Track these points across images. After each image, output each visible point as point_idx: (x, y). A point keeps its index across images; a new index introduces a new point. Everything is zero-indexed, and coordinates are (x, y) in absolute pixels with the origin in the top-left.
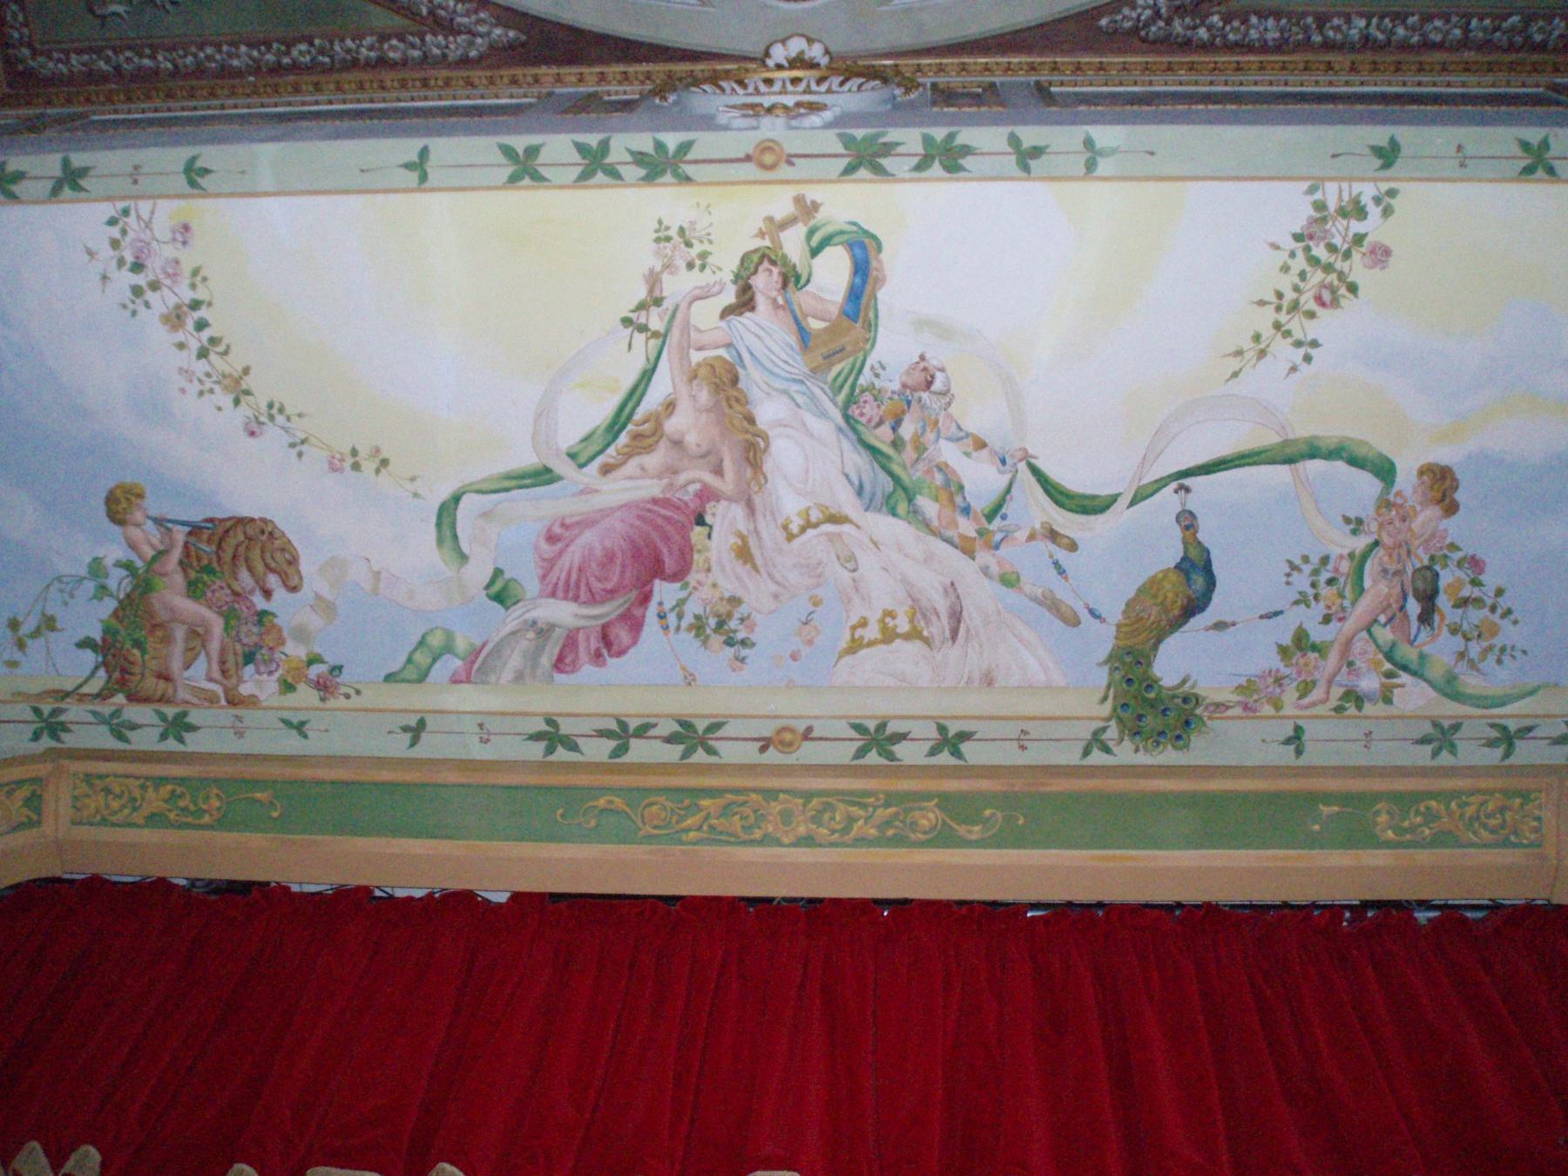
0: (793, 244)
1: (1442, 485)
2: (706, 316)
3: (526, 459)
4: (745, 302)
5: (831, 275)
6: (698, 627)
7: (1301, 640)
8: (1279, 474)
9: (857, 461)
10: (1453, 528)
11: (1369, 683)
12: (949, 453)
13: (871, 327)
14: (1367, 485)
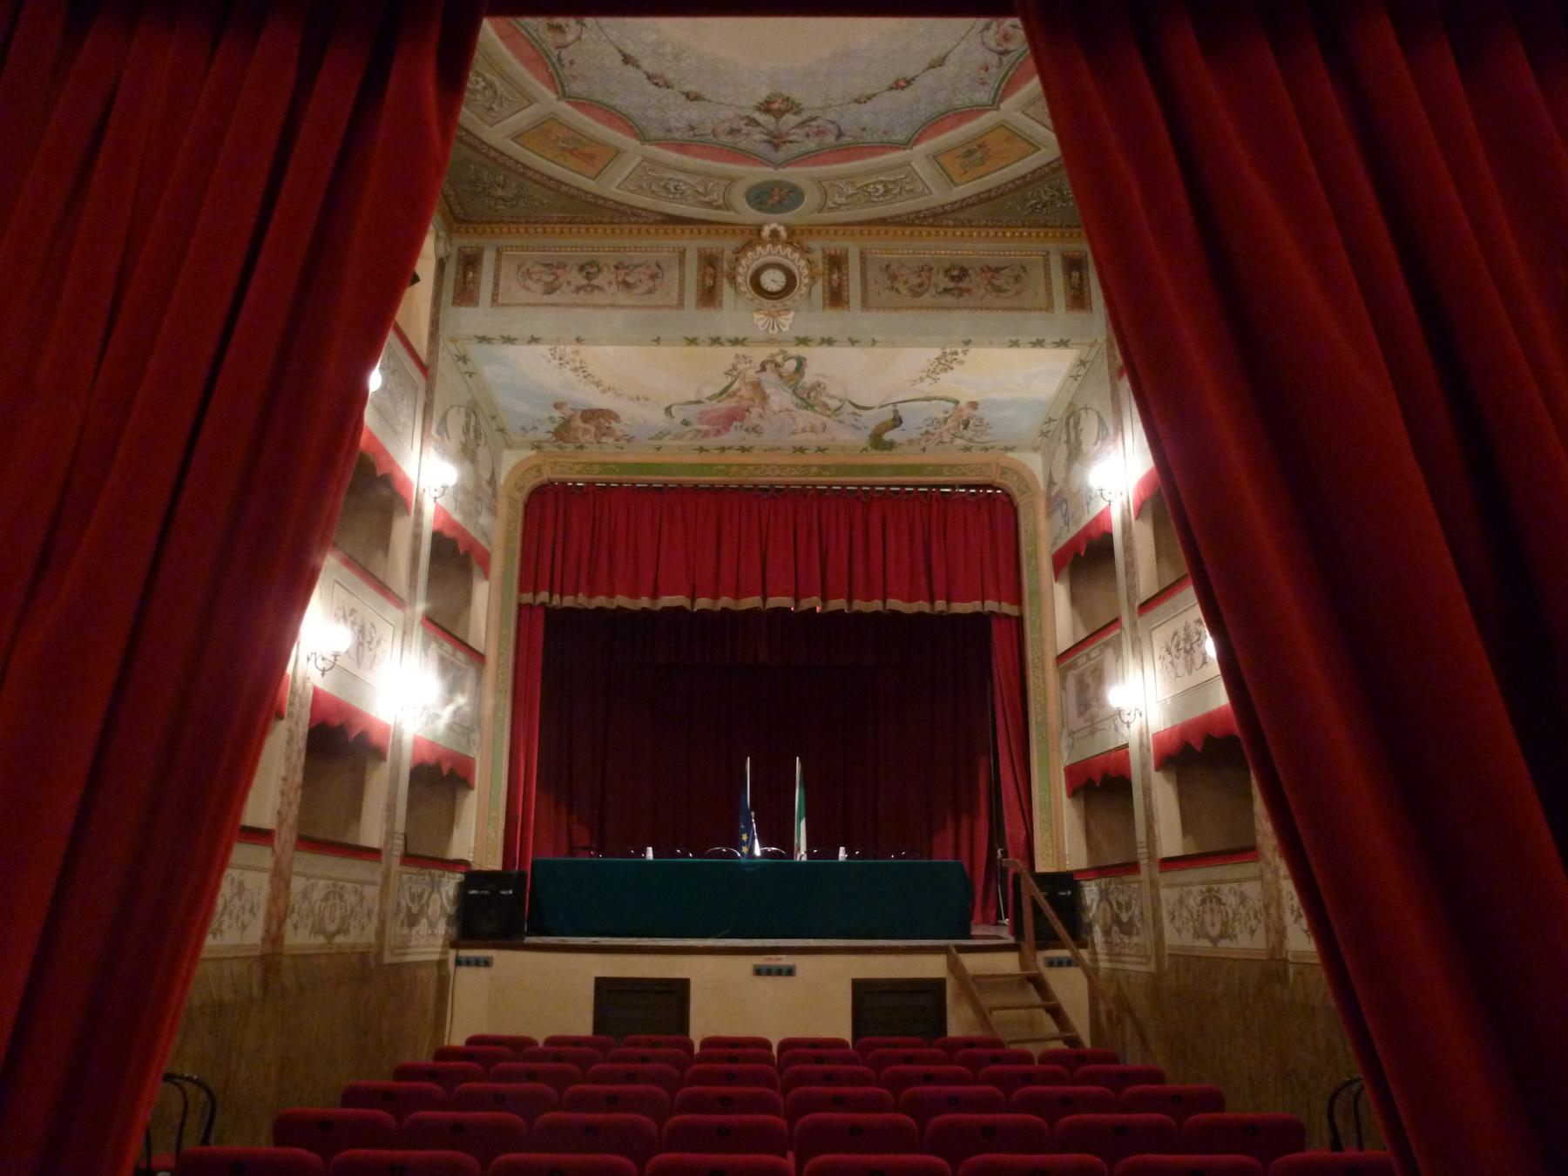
0: (779, 359)
1: (974, 405)
2: (751, 374)
3: (694, 398)
4: (763, 368)
5: (791, 365)
7: (927, 432)
9: (795, 400)
11: (947, 438)
12: (824, 399)
13: (802, 376)
14: (952, 405)
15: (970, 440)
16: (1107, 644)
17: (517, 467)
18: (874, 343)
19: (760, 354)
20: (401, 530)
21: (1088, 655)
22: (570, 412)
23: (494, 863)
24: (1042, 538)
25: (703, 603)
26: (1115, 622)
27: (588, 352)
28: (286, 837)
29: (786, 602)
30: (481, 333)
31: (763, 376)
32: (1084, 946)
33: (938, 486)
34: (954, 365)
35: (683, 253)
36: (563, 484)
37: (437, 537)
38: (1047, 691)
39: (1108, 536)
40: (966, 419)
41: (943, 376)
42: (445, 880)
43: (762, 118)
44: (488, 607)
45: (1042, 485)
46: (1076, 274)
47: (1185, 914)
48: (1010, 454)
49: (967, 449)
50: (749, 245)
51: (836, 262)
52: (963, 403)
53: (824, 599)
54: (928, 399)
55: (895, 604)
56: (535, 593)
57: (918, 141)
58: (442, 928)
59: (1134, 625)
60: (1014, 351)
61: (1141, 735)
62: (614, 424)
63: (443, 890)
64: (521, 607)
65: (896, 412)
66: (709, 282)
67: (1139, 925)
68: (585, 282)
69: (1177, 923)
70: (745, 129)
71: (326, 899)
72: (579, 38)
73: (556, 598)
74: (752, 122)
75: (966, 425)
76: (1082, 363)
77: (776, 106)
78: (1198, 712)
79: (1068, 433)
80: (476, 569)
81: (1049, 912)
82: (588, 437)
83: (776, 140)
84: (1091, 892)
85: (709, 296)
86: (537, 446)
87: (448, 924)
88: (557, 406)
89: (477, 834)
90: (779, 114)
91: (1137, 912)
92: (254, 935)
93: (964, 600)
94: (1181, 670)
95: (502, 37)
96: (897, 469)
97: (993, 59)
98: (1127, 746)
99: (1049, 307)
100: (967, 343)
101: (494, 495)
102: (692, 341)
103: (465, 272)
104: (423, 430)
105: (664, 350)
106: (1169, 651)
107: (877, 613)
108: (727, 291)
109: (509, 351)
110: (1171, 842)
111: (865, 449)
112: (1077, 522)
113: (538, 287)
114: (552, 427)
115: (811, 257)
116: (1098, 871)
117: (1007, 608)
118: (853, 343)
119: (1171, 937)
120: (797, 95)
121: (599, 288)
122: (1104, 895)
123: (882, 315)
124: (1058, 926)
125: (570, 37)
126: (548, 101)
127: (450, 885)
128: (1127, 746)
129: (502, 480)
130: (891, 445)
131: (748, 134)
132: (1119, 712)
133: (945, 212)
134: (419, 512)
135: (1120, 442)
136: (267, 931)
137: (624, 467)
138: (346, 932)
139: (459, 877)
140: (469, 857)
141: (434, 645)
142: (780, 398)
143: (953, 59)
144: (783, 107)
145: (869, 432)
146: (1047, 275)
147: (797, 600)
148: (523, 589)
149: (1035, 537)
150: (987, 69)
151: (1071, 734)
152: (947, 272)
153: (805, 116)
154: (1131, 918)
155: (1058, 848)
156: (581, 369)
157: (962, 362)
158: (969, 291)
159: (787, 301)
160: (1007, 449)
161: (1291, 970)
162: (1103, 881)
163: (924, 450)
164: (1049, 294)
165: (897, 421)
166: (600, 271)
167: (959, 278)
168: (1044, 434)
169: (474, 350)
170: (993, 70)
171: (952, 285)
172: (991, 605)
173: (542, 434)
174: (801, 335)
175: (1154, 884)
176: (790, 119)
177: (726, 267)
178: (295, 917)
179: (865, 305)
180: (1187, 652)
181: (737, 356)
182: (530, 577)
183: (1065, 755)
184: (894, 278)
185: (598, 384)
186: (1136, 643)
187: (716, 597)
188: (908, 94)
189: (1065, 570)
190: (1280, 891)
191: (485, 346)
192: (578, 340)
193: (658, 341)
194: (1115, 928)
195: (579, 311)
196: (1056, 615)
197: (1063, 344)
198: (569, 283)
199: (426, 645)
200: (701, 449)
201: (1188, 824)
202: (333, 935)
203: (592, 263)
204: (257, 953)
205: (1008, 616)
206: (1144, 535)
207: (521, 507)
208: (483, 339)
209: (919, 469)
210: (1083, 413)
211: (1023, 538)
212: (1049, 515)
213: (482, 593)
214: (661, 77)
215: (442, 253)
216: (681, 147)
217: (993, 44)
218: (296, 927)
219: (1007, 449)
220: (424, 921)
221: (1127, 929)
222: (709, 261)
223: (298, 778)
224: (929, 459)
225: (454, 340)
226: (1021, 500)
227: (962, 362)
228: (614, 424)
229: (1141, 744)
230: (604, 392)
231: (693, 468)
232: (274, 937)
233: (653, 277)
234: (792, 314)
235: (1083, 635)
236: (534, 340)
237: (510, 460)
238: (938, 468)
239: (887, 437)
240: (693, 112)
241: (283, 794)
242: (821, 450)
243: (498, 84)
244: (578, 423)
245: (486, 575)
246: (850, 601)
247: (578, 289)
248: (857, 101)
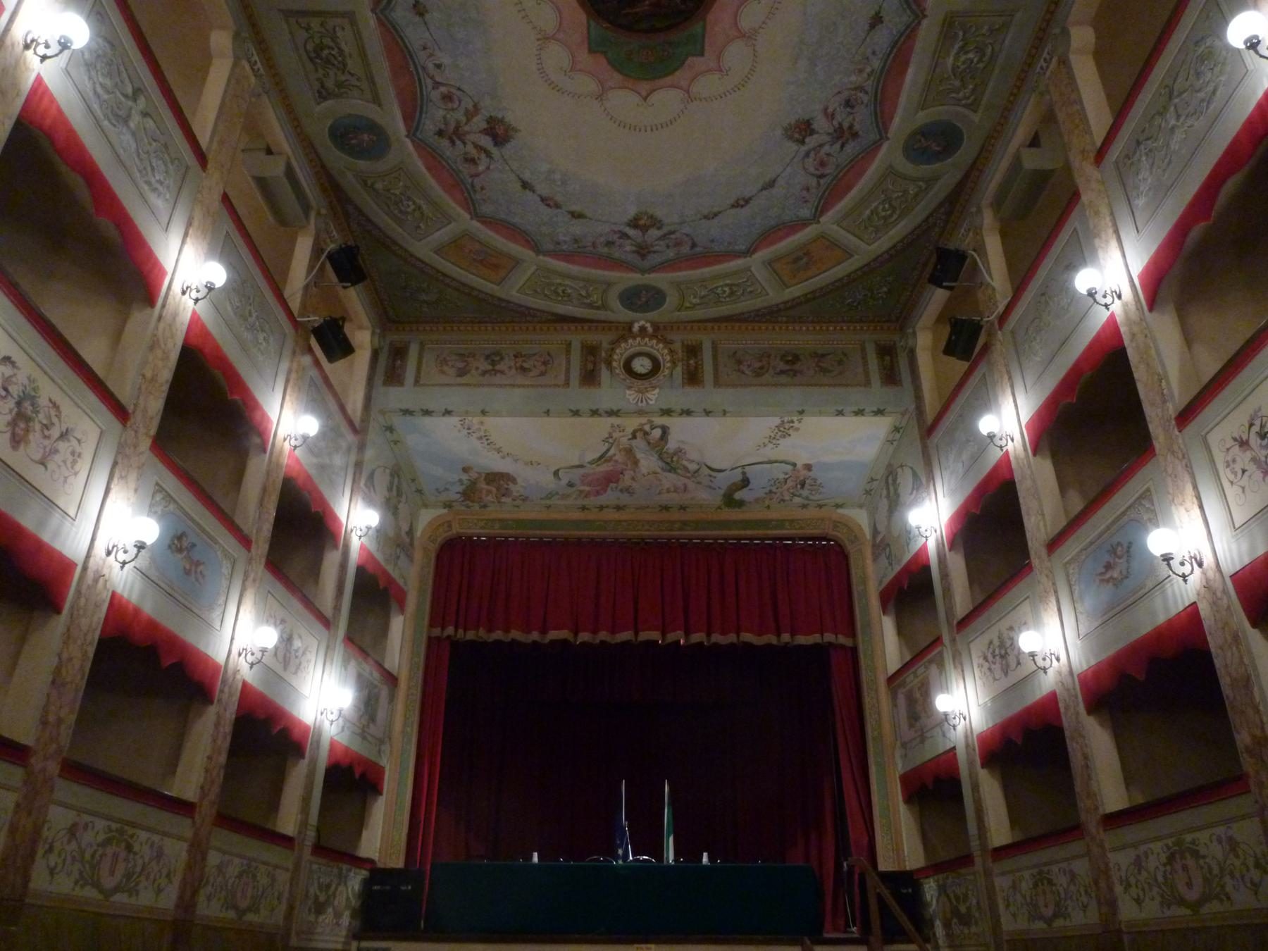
0: (647, 428)
1: (808, 467)
2: (624, 440)
3: (577, 463)
4: (634, 437)
5: (657, 433)
6: (621, 491)
8: (768, 466)
9: (661, 463)
10: (810, 474)
11: (787, 498)
12: (685, 463)
13: (666, 442)
14: (790, 467)
15: (807, 498)
16: (930, 662)
17: (430, 523)
18: (725, 413)
19: (632, 423)
20: (331, 561)
21: (915, 673)
22: (474, 475)
23: (398, 862)
24: (871, 577)
25: (584, 637)
26: (937, 641)
27: (490, 421)
28: (207, 811)
29: (654, 635)
30: (404, 407)
31: (634, 442)
32: (927, 940)
33: (782, 539)
34: (791, 432)
35: (569, 345)
36: (470, 538)
37: (361, 570)
38: (881, 709)
39: (926, 568)
40: (803, 479)
41: (782, 442)
42: (352, 874)
43: (631, 232)
44: (401, 637)
45: (868, 536)
46: (888, 358)
47: (1019, 897)
48: (840, 511)
49: (804, 506)
50: (623, 338)
51: (693, 351)
52: (799, 466)
53: (687, 634)
54: (770, 462)
55: (747, 637)
56: (443, 628)
57: (755, 251)
58: (346, 920)
59: (953, 640)
60: (840, 419)
61: (966, 737)
62: (511, 486)
63: (350, 883)
64: (430, 638)
65: (744, 473)
66: (590, 366)
67: (977, 915)
68: (490, 367)
69: (1012, 909)
70: (619, 242)
71: (240, 876)
72: (488, 168)
73: (461, 631)
74: (624, 235)
75: (803, 485)
76: (897, 429)
77: (642, 222)
78: (1017, 708)
79: (888, 489)
80: (394, 606)
81: (892, 903)
82: (490, 498)
83: (643, 251)
84: (930, 889)
85: (590, 378)
86: (448, 505)
87: (352, 917)
88: (465, 470)
89: (383, 834)
90: (645, 229)
91: (974, 901)
92: (168, 900)
93: (806, 634)
94: (998, 673)
95: (429, 169)
96: (747, 524)
97: (813, 182)
98: (954, 748)
99: (868, 383)
100: (801, 412)
101: (412, 544)
102: (576, 413)
103: (394, 360)
104: (354, 481)
105: (553, 421)
106: (986, 659)
107: (732, 644)
108: (605, 374)
109: (427, 420)
110: (1000, 831)
111: (719, 508)
112: (900, 561)
113: (452, 372)
114: (460, 489)
115: (672, 347)
116: (935, 868)
117: (842, 640)
118: (708, 413)
119: (1007, 924)
120: (659, 213)
121: (502, 372)
122: (942, 889)
123: (730, 391)
124: (904, 920)
125: (481, 168)
126: (463, 220)
127: (356, 880)
128: (954, 748)
129: (418, 533)
130: (741, 504)
131: (620, 246)
132: (946, 715)
133: (779, 310)
134: (347, 547)
135: (932, 488)
136: (181, 898)
137: (520, 523)
138: (257, 911)
139: (364, 873)
140: (375, 855)
141: (353, 663)
142: (648, 462)
143: (780, 181)
144: (648, 223)
145: (722, 492)
146: (864, 358)
147: (664, 635)
148: (432, 624)
149: (864, 581)
150: (808, 189)
151: (904, 745)
152: (783, 358)
153: (665, 230)
154: (969, 909)
155: (898, 850)
156: (484, 438)
157: (798, 429)
158: (801, 372)
159: (654, 381)
160: (837, 506)
161: (1126, 938)
162: (941, 876)
163: (768, 507)
164: (867, 373)
165: (745, 482)
166: (502, 359)
167: (793, 362)
168: (868, 492)
169: (397, 421)
170: (814, 191)
171: (788, 367)
172: (829, 637)
173: (453, 495)
174: (665, 407)
175: (988, 874)
176: (654, 233)
177: (603, 354)
178: (209, 889)
179: (717, 383)
180: (1002, 657)
181: (612, 426)
182: (438, 616)
183: (900, 766)
184: (740, 362)
185: (499, 451)
186: (957, 657)
187: (595, 632)
188: (745, 212)
189: (891, 607)
190: (1107, 864)
191: (408, 418)
192: (483, 413)
193: (548, 413)
194: (955, 920)
195: (485, 390)
196: (886, 643)
197: (879, 412)
198: (477, 368)
199: (345, 663)
200: (584, 508)
201: (1015, 818)
202: (244, 912)
203: (498, 353)
204: (169, 919)
205: (843, 647)
206: (957, 564)
207: (433, 556)
208: (407, 412)
209: (765, 523)
210: (899, 470)
211: (854, 580)
212: (876, 558)
213: (398, 625)
214: (551, 199)
215: (377, 346)
216: (568, 257)
217: (812, 169)
218: (209, 899)
219: (837, 506)
220: (330, 910)
221: (965, 920)
222: (590, 351)
223: (223, 759)
224: (772, 515)
225: (383, 413)
226: (851, 549)
227: (798, 429)
228: (511, 486)
229: (967, 746)
230: (503, 458)
231: (576, 524)
232: (187, 903)
233: (545, 363)
234: (657, 391)
235: (908, 658)
236: (448, 413)
237: (426, 517)
238: (781, 523)
239: (738, 495)
240: (577, 228)
241: (207, 771)
242: (683, 508)
243: (424, 207)
244: (482, 485)
245: (402, 608)
246: (709, 635)
247: (484, 373)
248: (706, 217)
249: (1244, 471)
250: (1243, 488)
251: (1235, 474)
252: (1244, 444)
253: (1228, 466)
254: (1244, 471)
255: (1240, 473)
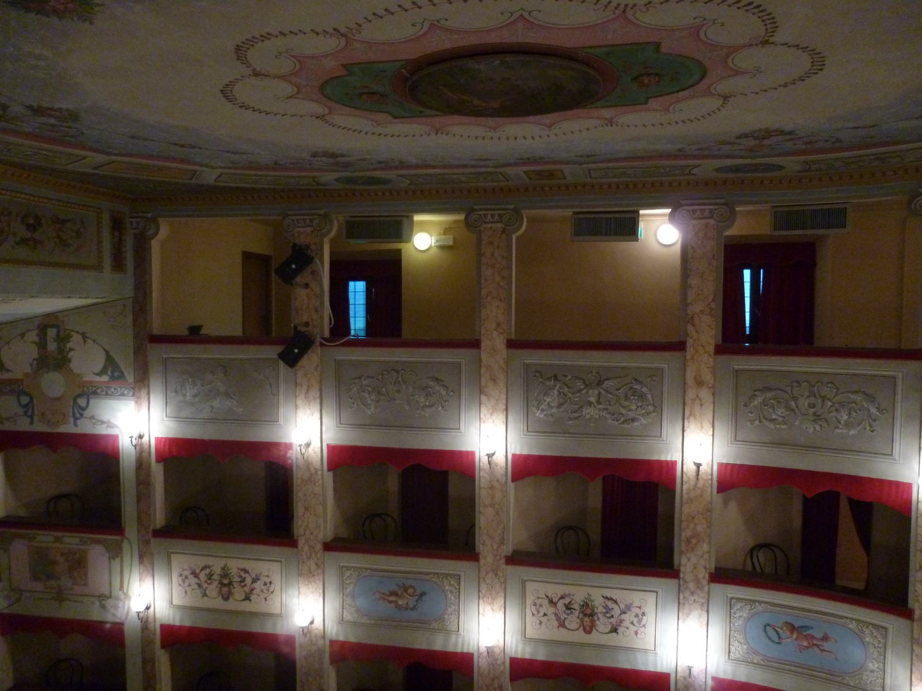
16: (98, 542)
99: (99, 268)
171: (28, 235)
249: (545, 615)
250: (541, 623)
251: (539, 612)
252: (551, 602)
253: (535, 605)
254: (545, 615)
255: (542, 614)
